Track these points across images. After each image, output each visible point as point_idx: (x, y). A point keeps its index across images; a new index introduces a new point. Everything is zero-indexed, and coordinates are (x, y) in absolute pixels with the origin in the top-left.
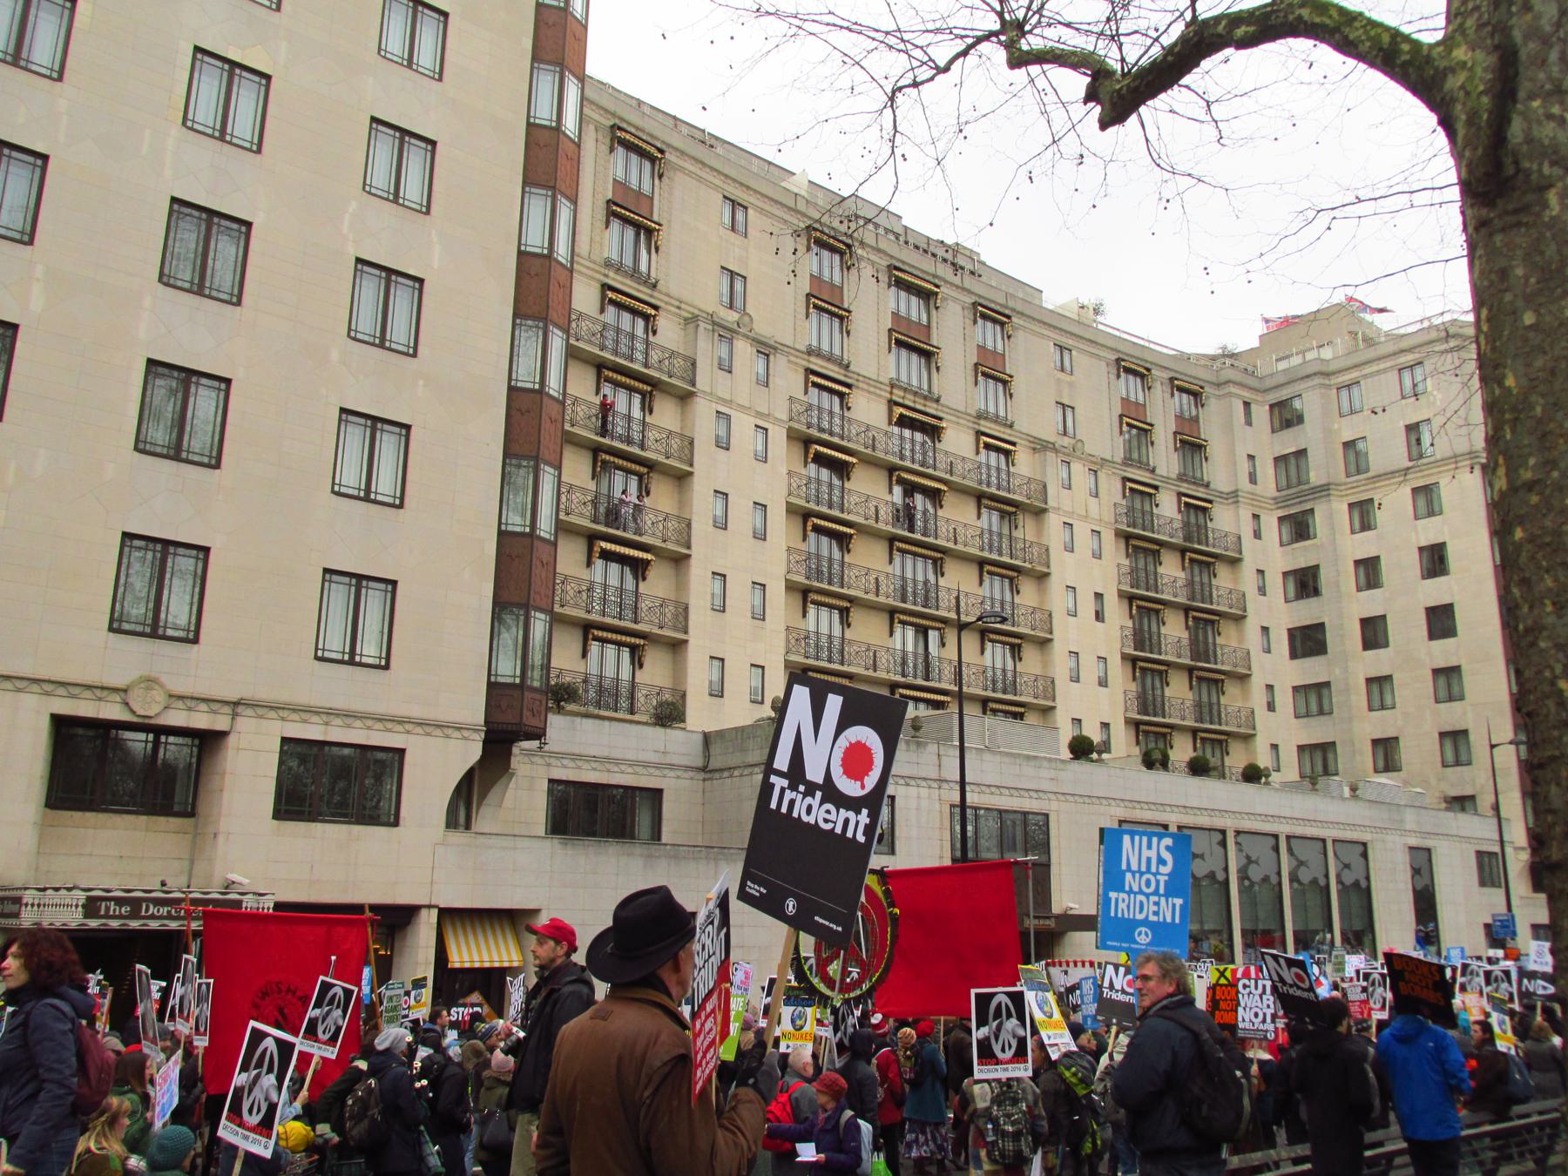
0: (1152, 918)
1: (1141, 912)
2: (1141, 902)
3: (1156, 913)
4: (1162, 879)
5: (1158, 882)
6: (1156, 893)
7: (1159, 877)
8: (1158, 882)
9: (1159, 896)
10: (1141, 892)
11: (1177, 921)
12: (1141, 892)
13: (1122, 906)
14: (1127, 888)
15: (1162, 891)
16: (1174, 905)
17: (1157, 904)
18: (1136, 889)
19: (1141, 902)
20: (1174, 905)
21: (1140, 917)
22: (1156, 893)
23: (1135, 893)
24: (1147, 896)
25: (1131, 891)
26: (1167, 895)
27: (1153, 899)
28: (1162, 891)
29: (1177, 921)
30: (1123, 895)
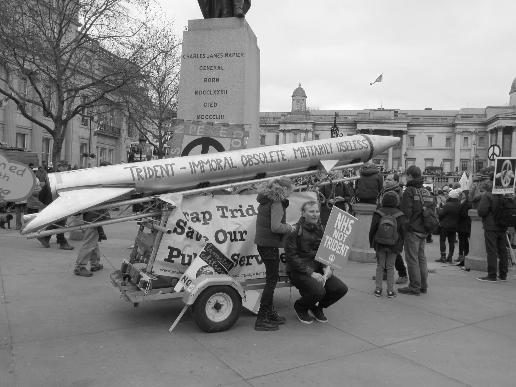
0: (337, 252)
1: (335, 248)
2: (336, 244)
3: (339, 250)
4: (346, 236)
5: (344, 237)
6: (342, 242)
7: (345, 235)
8: (344, 237)
9: (343, 243)
10: (337, 240)
11: (345, 256)
12: (337, 240)
13: (329, 243)
14: (333, 236)
15: (344, 242)
16: (346, 249)
17: (341, 246)
18: (336, 238)
19: (336, 244)
20: (346, 249)
21: (334, 250)
22: (342, 242)
23: (336, 239)
24: (339, 241)
25: (334, 238)
26: (345, 244)
27: (340, 244)
28: (344, 242)
29: (345, 256)
30: (331, 239)
